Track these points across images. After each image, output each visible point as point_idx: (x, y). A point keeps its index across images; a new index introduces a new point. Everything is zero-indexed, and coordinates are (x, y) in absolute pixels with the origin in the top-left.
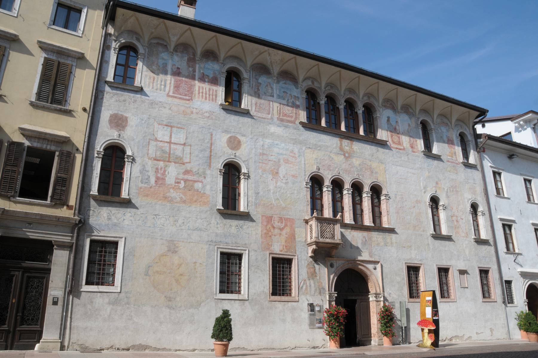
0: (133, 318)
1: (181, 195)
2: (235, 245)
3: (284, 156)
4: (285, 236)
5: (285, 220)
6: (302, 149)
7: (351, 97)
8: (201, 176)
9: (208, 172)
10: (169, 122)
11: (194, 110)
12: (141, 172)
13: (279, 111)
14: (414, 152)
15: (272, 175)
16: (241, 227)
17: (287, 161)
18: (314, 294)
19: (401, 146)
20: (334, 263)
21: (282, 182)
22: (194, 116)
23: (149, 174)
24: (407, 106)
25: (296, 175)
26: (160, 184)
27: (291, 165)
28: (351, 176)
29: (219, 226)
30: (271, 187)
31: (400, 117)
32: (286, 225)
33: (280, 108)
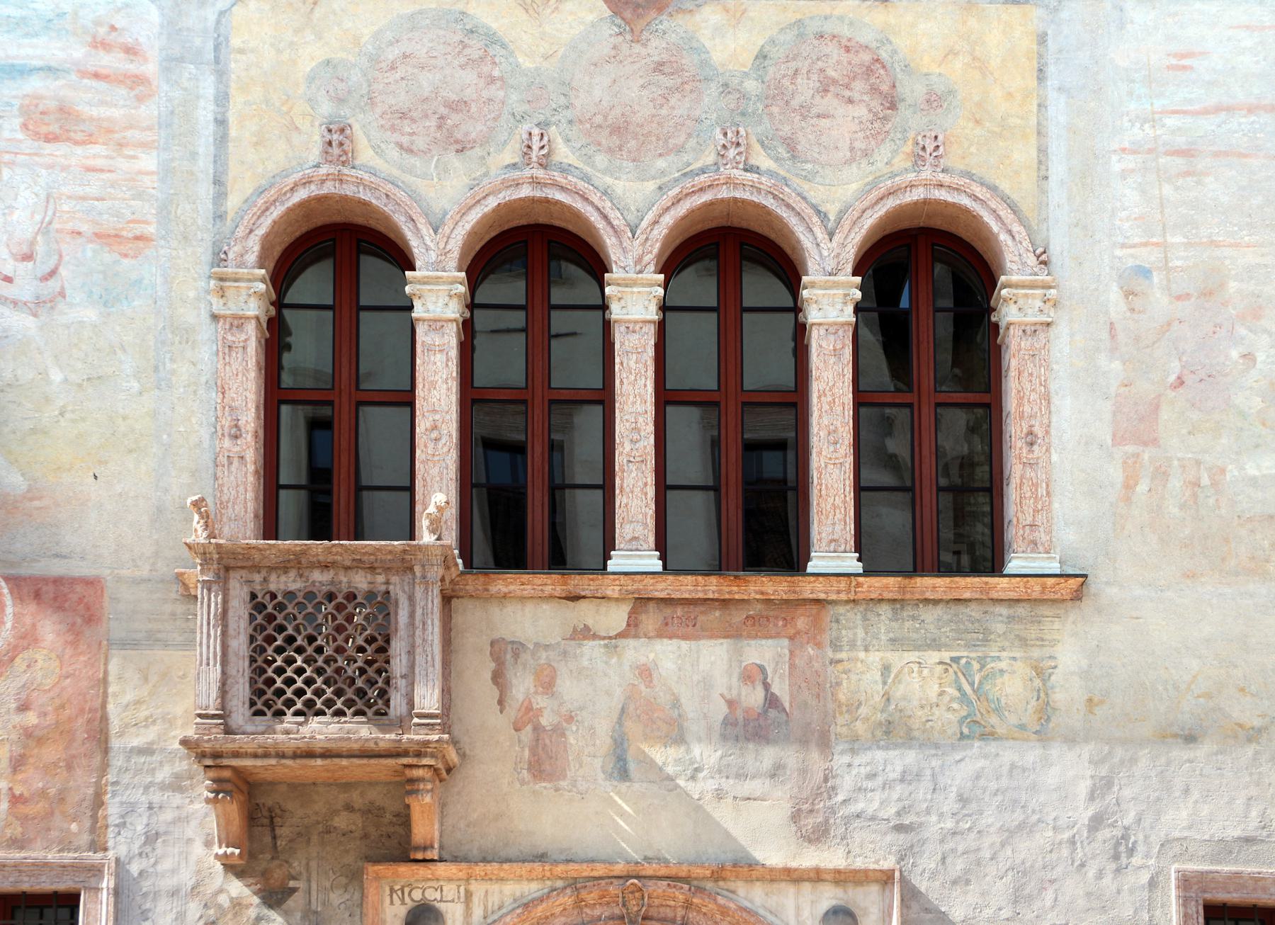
3: (35, 84)
4: (17, 719)
20: (442, 907)
25: (139, 229)
27: (97, 153)
28: (661, 163)
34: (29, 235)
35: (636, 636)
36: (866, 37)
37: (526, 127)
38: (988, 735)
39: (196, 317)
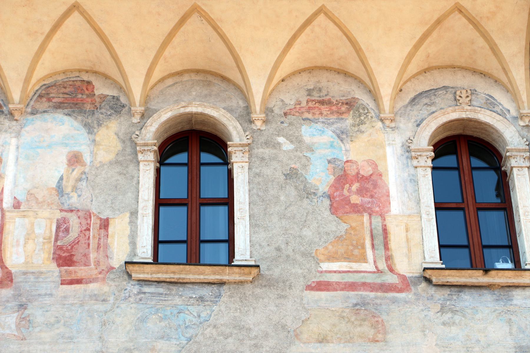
24: (85, 78)
31: (18, 135)
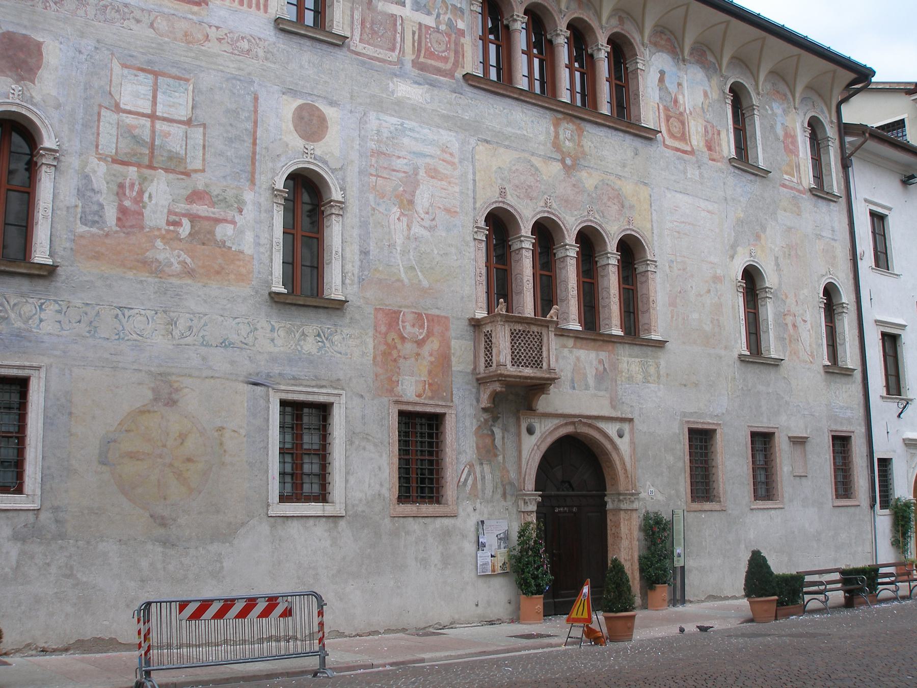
0: (75, 572)
1: (184, 256)
2: (314, 383)
3: (428, 160)
4: (429, 358)
5: (428, 321)
6: (469, 144)
7: (581, 16)
8: (232, 206)
9: (248, 196)
10: (149, 62)
11: (212, 32)
12: (80, 193)
13: (416, 44)
14: (713, 160)
15: (400, 208)
16: (327, 339)
17: (433, 173)
18: (492, 496)
19: (687, 143)
20: (535, 424)
21: (421, 226)
22: (213, 47)
23: (101, 200)
25: (455, 209)
26: (131, 227)
28: (576, 213)
29: (276, 334)
30: (399, 240)
31: (686, 74)
32: (430, 334)
33: (420, 37)
34: (427, 206)
35: (575, 348)
36: (617, 187)
37: (546, 196)
38: (648, 382)
39: (469, 238)
